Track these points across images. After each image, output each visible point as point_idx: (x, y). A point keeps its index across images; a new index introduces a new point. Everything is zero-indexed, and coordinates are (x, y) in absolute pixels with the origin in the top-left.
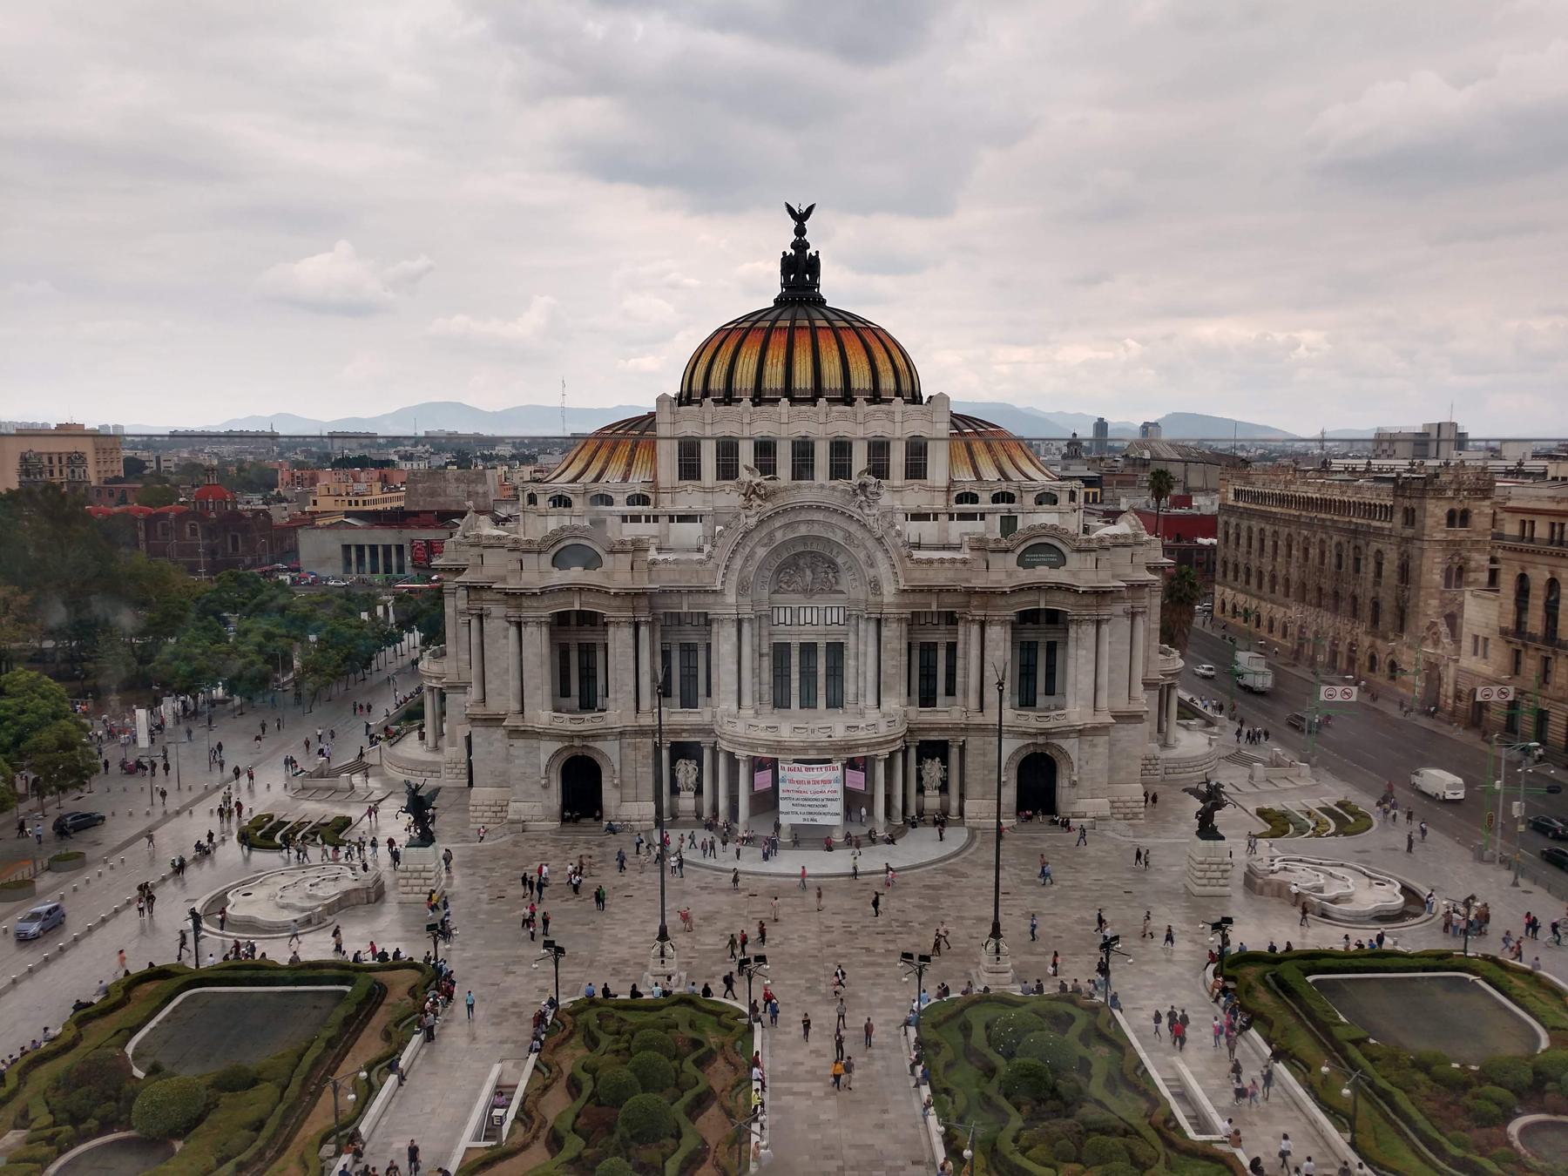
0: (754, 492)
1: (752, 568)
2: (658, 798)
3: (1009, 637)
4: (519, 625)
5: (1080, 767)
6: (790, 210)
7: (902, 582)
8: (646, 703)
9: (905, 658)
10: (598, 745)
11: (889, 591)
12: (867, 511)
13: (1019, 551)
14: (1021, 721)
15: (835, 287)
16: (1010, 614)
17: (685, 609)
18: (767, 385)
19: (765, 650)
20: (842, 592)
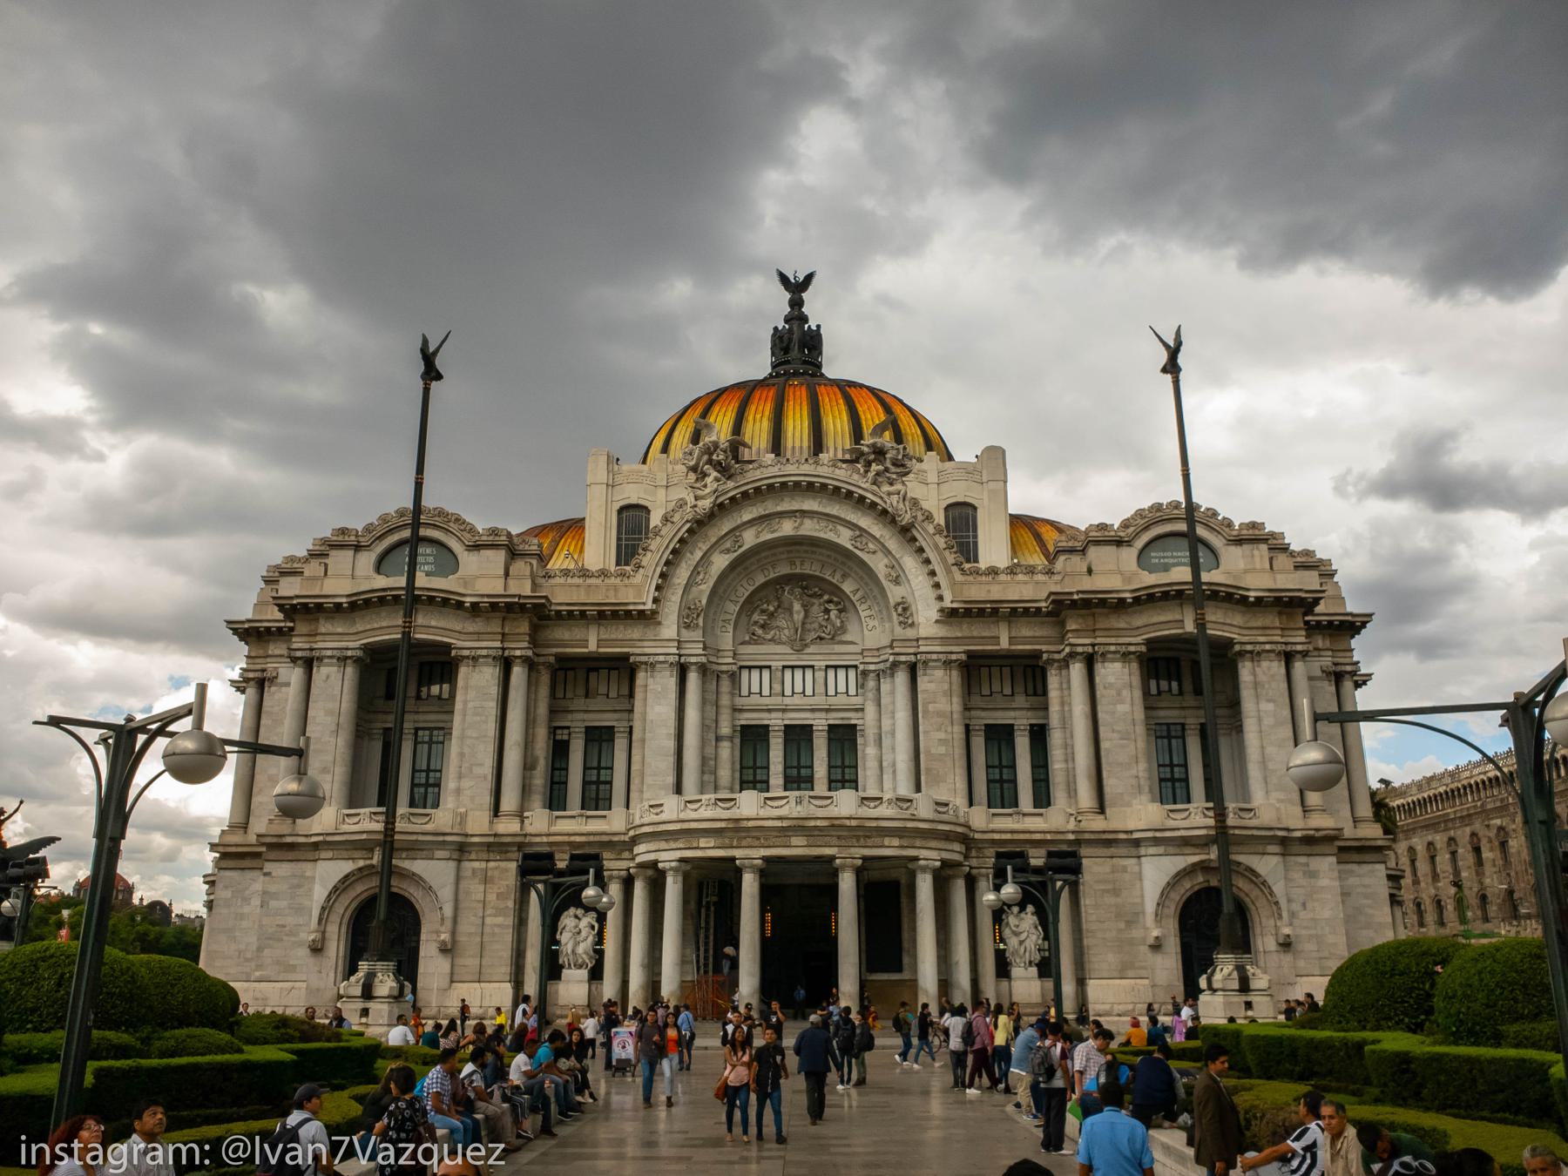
0: (710, 462)
2: (518, 983)
3: (1136, 680)
4: (309, 664)
5: (1293, 915)
6: (783, 278)
7: (948, 597)
8: (509, 801)
9: (958, 730)
10: (418, 866)
11: (926, 616)
12: (886, 488)
13: (1140, 543)
14: (1177, 821)
16: (1136, 642)
17: (592, 646)
19: (725, 730)
20: (852, 643)
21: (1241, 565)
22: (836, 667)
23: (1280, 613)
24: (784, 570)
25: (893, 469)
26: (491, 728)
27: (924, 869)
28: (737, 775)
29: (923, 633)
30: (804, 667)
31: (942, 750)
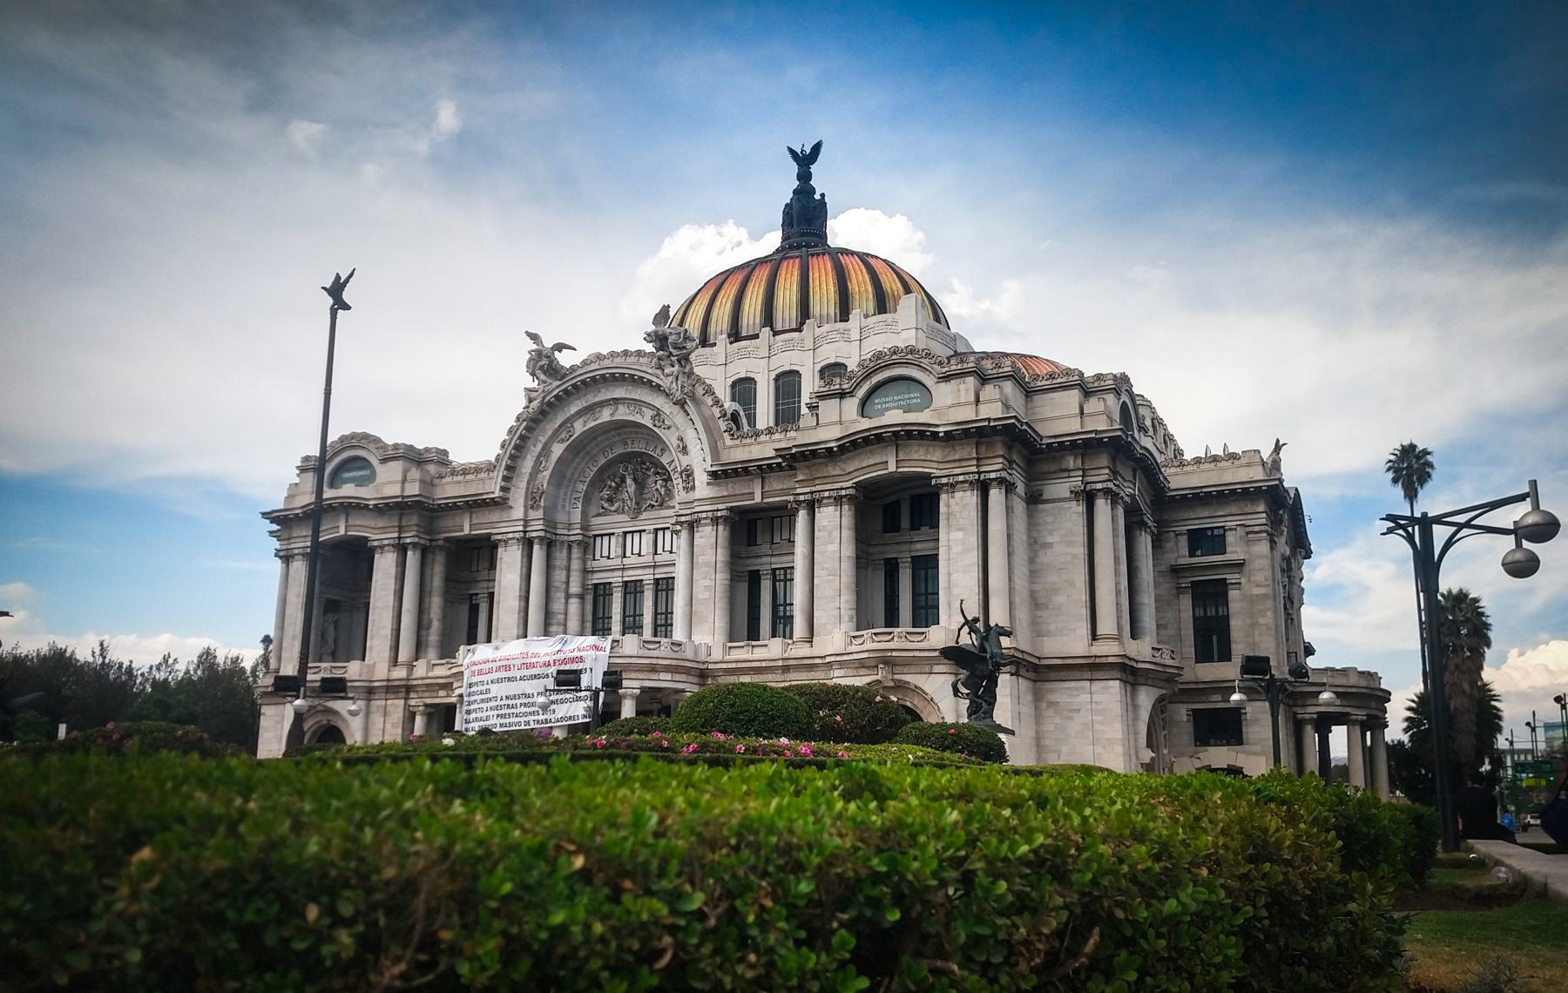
1: (547, 474)
11: (701, 478)
13: (861, 393)
15: (842, 231)
16: (846, 485)
17: (466, 531)
18: (712, 328)
19: (575, 588)
21: (949, 402)
22: (664, 529)
23: (978, 445)
24: (619, 450)
25: (675, 352)
26: (390, 600)
27: (625, 696)
28: (589, 625)
29: (698, 494)
30: (640, 531)
31: (706, 595)
